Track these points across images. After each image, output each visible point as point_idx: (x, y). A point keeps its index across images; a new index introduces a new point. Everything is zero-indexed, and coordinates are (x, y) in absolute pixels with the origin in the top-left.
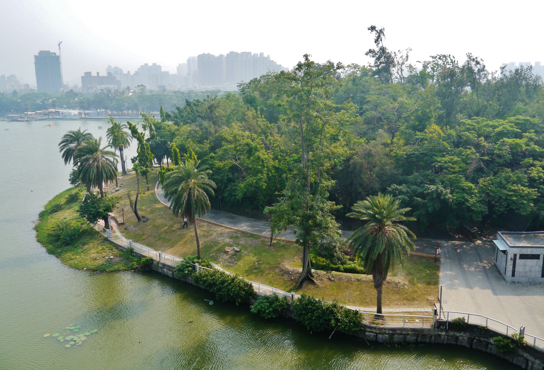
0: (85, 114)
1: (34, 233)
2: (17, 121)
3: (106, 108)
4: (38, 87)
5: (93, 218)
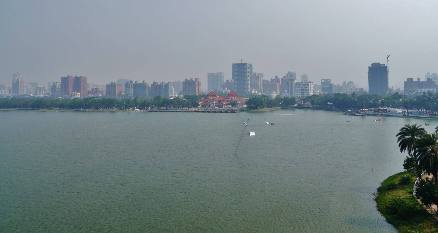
0: (408, 113)
1: (375, 203)
2: (355, 115)
3: (428, 108)
4: (369, 90)
5: (428, 201)
